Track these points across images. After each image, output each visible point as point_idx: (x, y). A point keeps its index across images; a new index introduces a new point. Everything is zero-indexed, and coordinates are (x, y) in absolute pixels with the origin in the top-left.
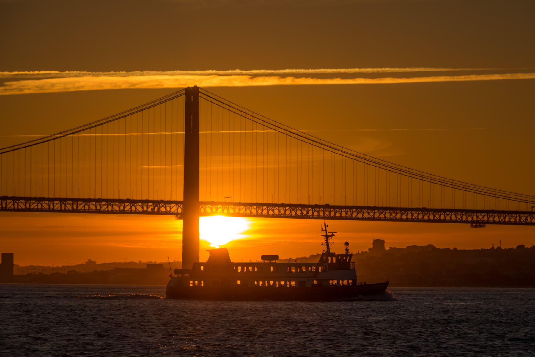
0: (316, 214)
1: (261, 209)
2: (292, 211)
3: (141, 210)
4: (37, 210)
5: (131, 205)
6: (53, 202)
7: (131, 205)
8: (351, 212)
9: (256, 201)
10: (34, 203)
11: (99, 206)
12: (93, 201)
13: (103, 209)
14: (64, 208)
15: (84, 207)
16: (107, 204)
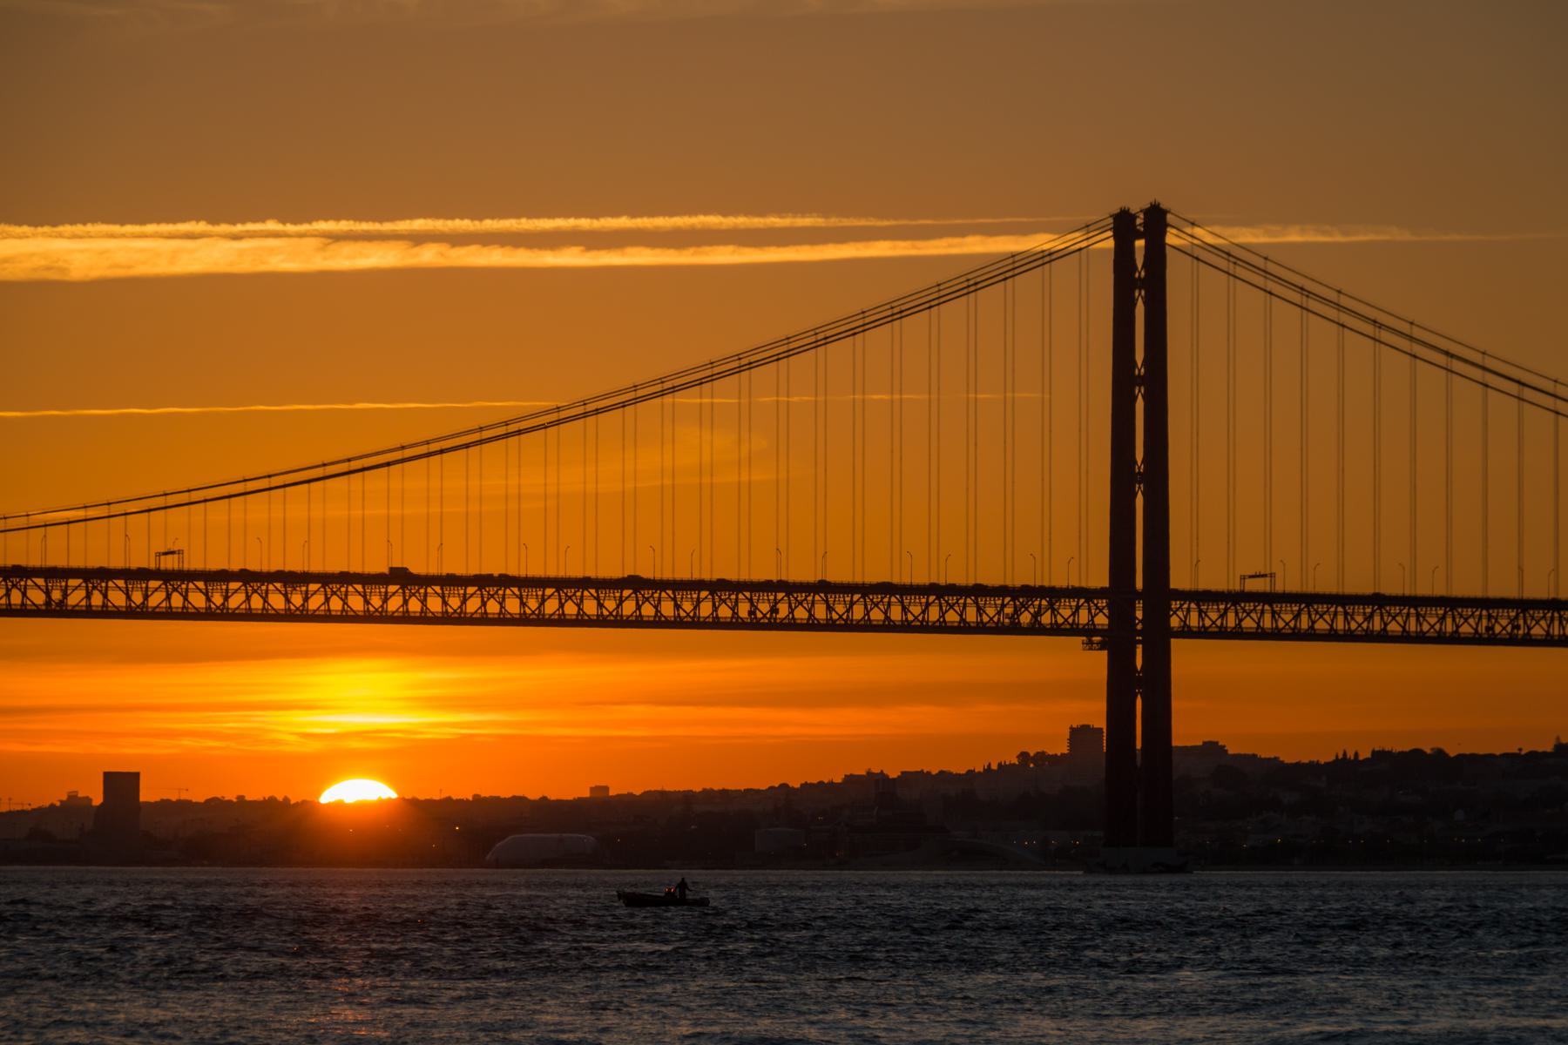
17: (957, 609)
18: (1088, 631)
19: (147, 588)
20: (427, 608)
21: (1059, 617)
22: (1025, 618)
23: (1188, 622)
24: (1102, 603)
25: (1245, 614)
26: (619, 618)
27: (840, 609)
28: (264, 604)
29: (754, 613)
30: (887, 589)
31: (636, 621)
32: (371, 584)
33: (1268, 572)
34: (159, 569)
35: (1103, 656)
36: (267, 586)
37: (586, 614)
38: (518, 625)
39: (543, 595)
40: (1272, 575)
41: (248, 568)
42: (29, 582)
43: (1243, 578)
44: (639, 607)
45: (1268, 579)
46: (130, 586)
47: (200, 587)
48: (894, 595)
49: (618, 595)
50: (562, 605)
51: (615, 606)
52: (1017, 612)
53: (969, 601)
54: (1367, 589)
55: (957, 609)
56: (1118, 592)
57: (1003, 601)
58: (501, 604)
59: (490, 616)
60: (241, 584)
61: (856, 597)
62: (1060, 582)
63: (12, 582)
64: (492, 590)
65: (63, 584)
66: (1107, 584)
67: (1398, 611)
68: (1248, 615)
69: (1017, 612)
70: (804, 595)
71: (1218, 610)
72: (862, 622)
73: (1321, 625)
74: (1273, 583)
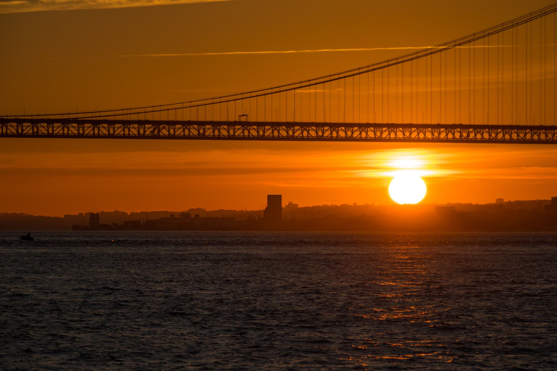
0: (421, 136)
1: (466, 132)
2: (477, 133)
3: (257, 135)
4: (244, 138)
5: (243, 128)
6: (174, 127)
7: (243, 128)
8: (466, 132)
9: (460, 121)
10: (180, 128)
11: (261, 131)
12: (224, 125)
13: (237, 134)
14: (218, 134)
15: (243, 132)
16: (272, 129)
26: (525, 140)
31: (475, 140)
37: (484, 138)
39: (497, 132)
44: (532, 136)
46: (490, 131)
49: (524, 131)
51: (523, 136)
59: (506, 140)
60: (181, 125)
63: (304, 128)
64: (535, 131)
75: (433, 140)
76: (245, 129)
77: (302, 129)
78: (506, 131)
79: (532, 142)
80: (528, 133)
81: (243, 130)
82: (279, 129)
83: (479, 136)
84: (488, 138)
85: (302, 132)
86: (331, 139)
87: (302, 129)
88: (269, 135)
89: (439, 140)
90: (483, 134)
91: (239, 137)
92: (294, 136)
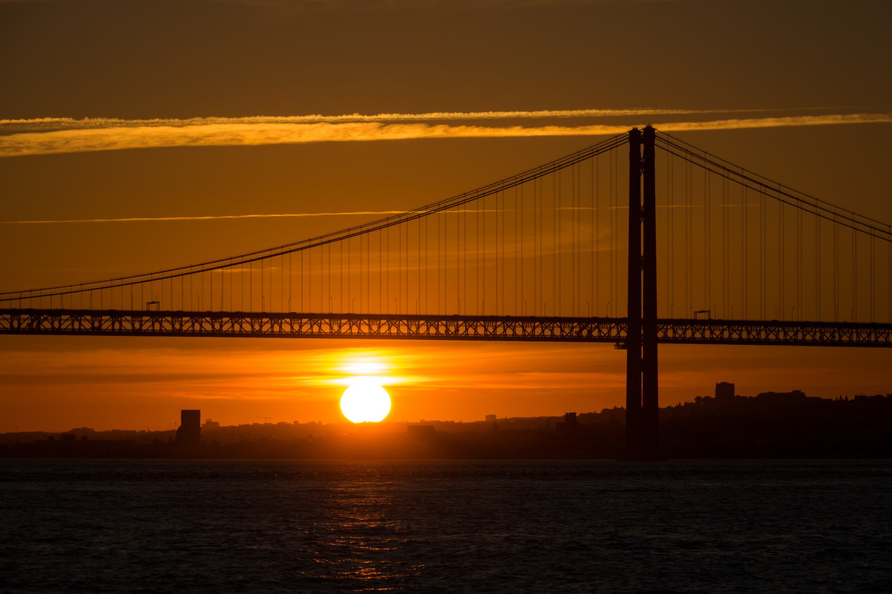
17: (737, 332)
18: (616, 340)
19: (301, 322)
20: (439, 332)
21: (714, 335)
22: (585, 333)
23: (815, 338)
24: (623, 325)
25: (879, 335)
27: (680, 332)
28: (398, 331)
29: (822, 337)
30: (775, 323)
32: (411, 320)
33: (707, 310)
34: (148, 310)
35: (625, 352)
36: (399, 322)
38: (464, 340)
40: (709, 312)
41: (876, 321)
42: (83, 318)
43: (696, 313)
45: (707, 313)
47: (288, 321)
48: (744, 326)
50: (505, 330)
52: (581, 331)
53: (743, 328)
54: (867, 320)
55: (737, 332)
56: (631, 321)
57: (797, 329)
58: (514, 330)
61: (613, 325)
62: (602, 315)
65: (100, 319)
66: (626, 316)
67: (883, 331)
68: (808, 333)
69: (581, 331)
70: (624, 325)
71: (682, 329)
72: (616, 338)
73: (809, 337)
74: (710, 315)
75: (409, 336)
76: (155, 321)
77: (232, 321)
78: (545, 325)
79: (542, 338)
80: (499, 326)
81: (153, 322)
82: (242, 322)
83: (433, 331)
84: (521, 334)
85: (233, 326)
86: (272, 335)
87: (232, 321)
88: (187, 330)
89: (418, 336)
90: (476, 328)
91: (346, 334)
92: (222, 331)
